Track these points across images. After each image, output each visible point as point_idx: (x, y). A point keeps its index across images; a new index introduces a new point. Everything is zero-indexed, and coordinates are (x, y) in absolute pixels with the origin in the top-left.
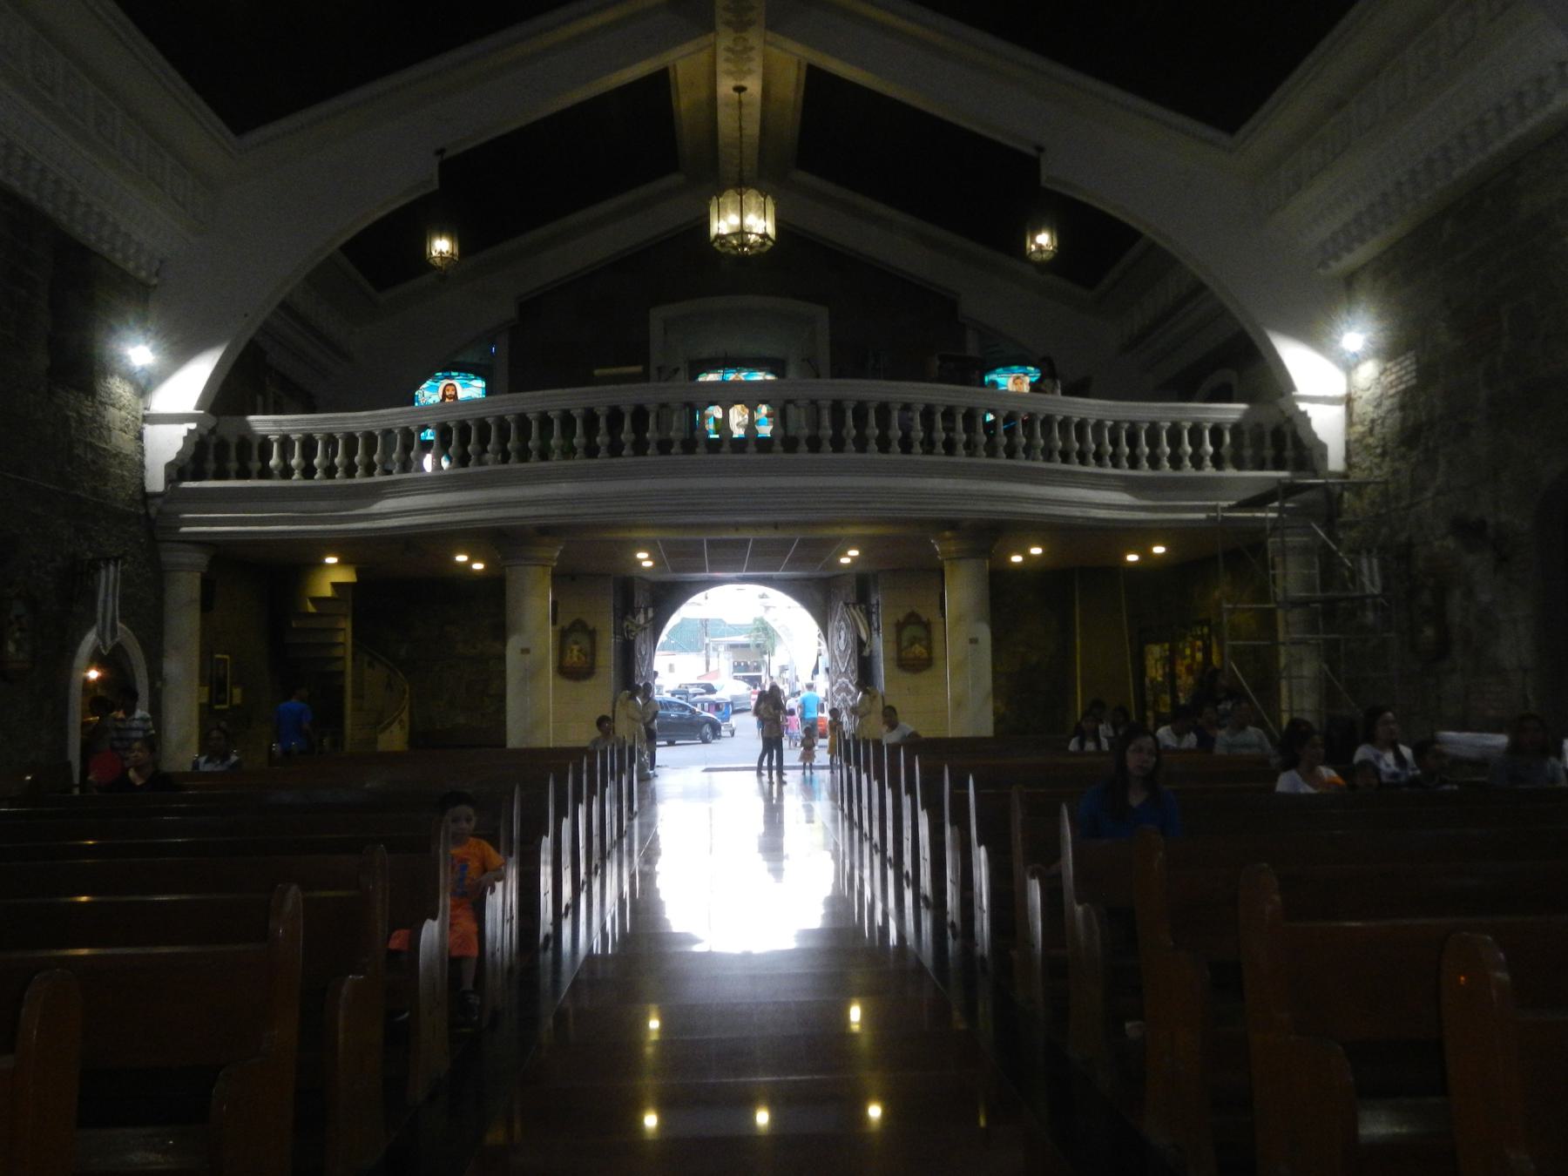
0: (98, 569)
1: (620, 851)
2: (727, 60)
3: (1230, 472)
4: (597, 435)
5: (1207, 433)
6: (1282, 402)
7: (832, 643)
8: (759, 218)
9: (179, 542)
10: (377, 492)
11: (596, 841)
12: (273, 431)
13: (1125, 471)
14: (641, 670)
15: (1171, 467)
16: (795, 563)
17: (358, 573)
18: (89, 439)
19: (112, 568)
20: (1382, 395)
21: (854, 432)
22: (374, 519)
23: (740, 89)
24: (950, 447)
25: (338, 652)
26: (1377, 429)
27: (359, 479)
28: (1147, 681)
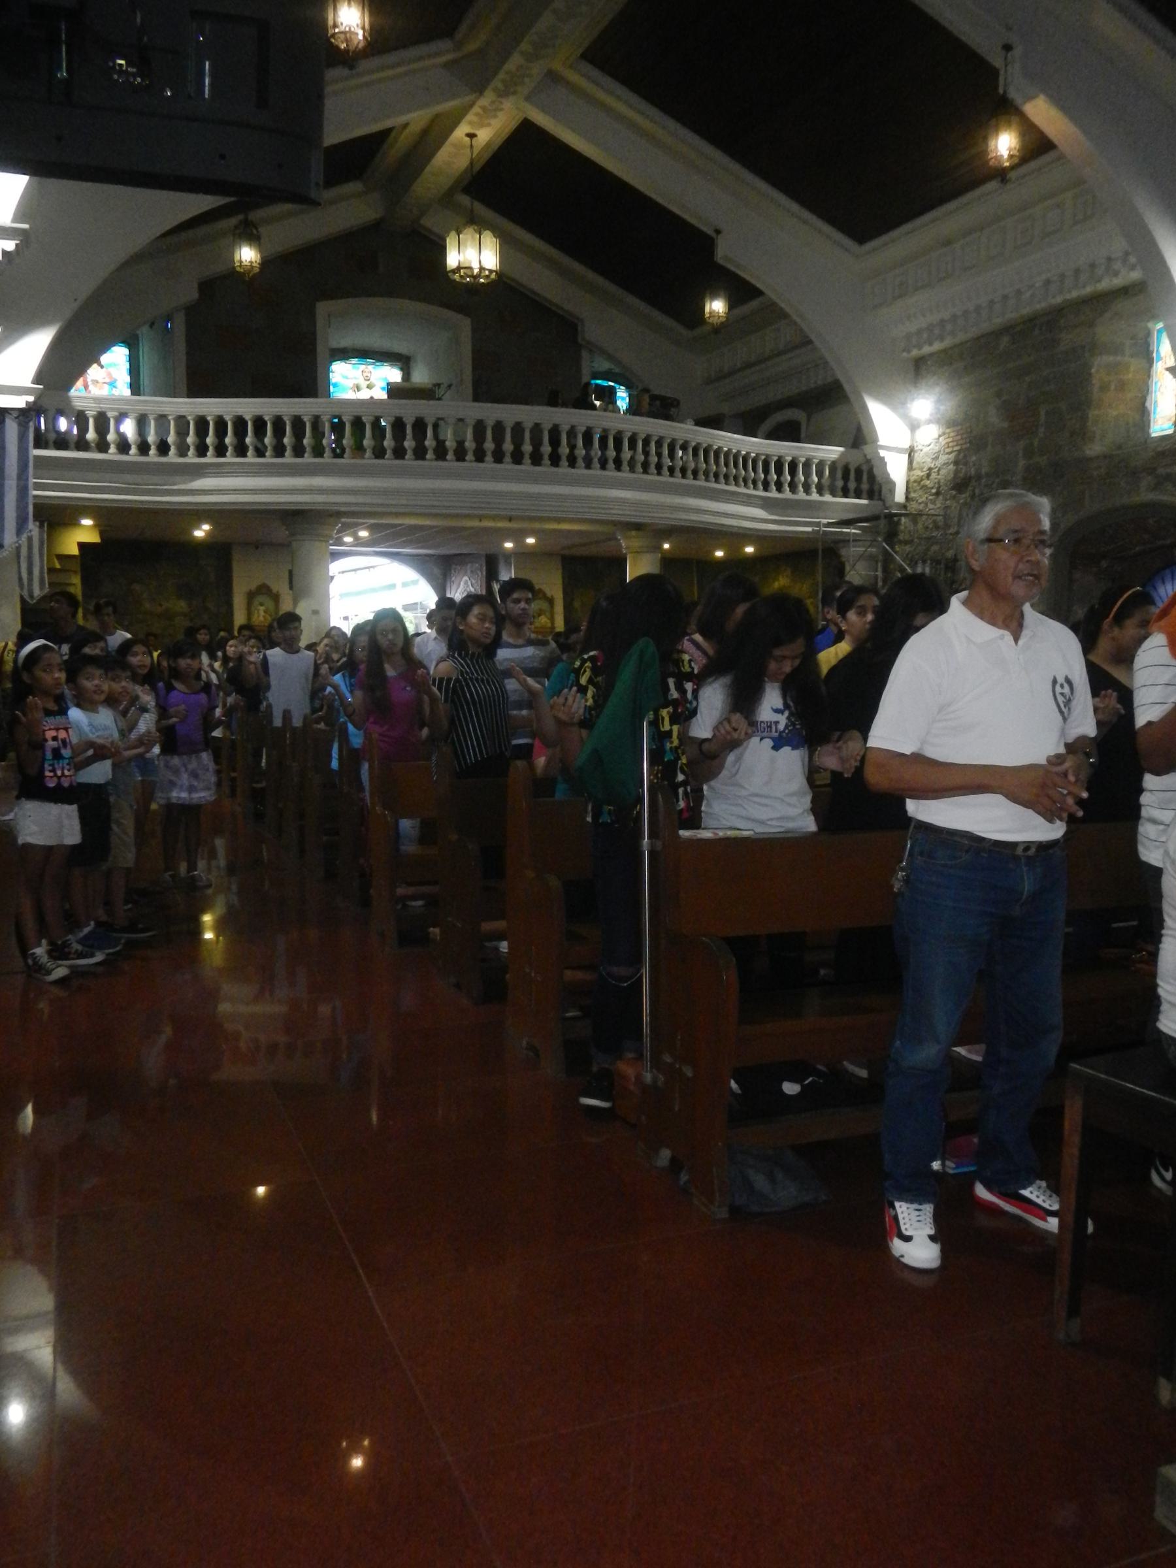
3: (828, 498)
10: (198, 471)
12: (92, 407)
15: (790, 491)
20: (940, 451)
22: (194, 495)
26: (933, 475)
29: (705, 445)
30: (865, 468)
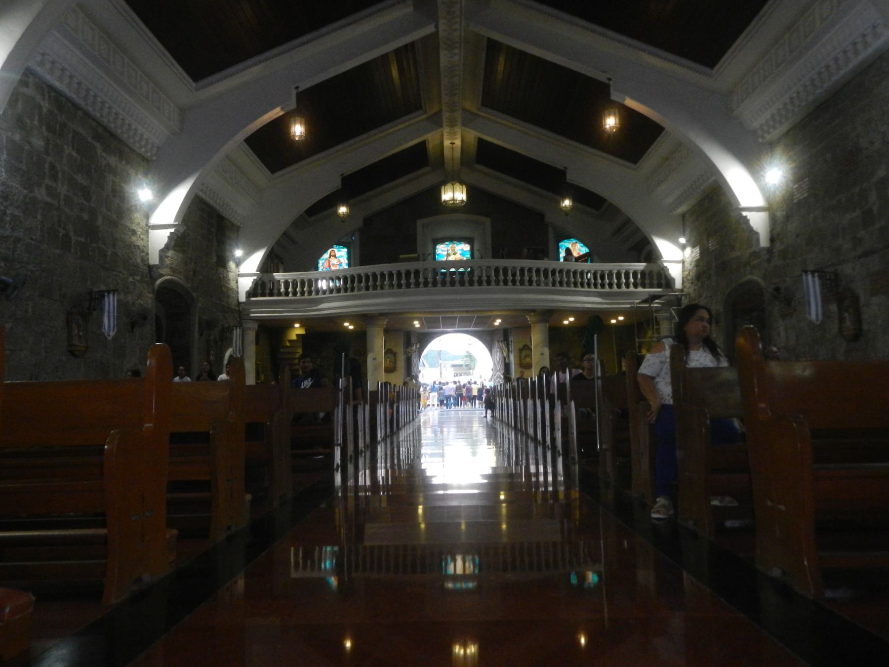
2: (448, 135)
3: (640, 289)
6: (659, 262)
7: (494, 357)
9: (249, 320)
10: (321, 301)
13: (599, 290)
14: (414, 369)
16: (476, 325)
17: (306, 330)
18: (226, 285)
19: (238, 330)
23: (452, 144)
26: (691, 274)
27: (313, 296)
29: (551, 269)
30: (662, 272)
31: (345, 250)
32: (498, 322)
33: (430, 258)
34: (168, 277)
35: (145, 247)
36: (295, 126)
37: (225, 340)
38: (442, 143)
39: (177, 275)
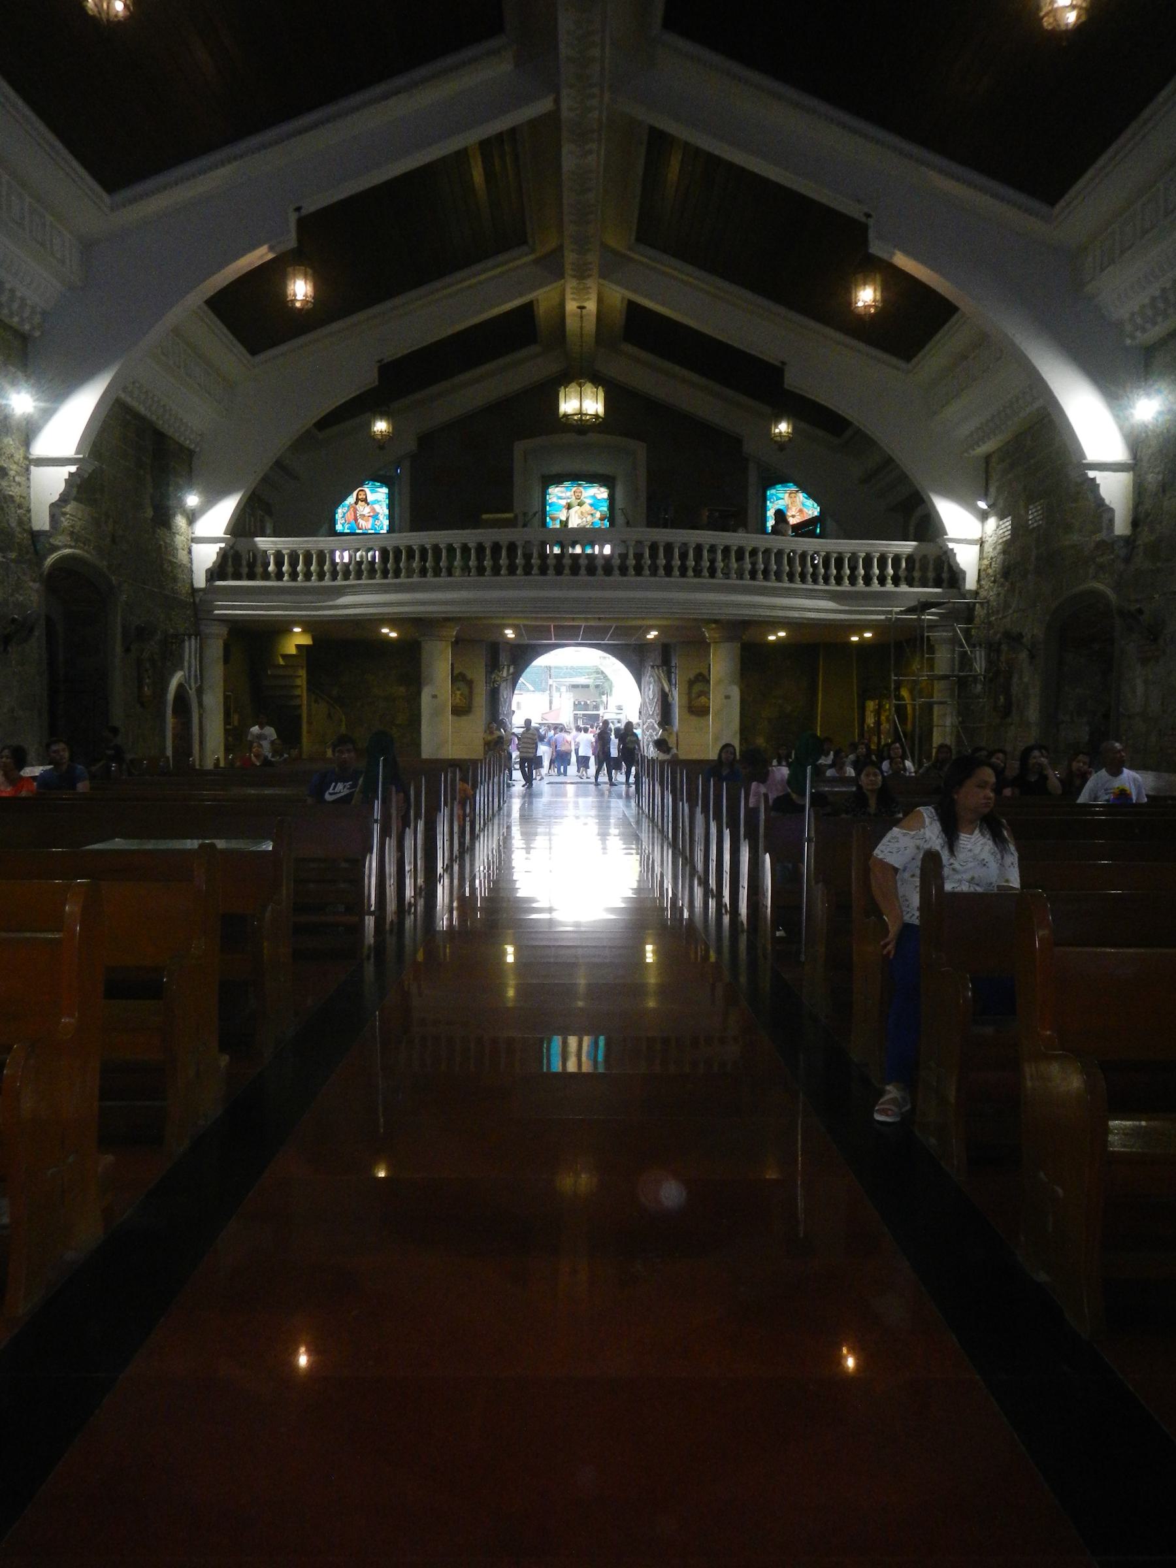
0: (183, 641)
1: (499, 814)
3: (904, 588)
4: (484, 560)
5: (890, 561)
7: (644, 694)
8: (594, 402)
9: (214, 620)
11: (491, 804)
13: (833, 587)
14: (503, 710)
17: (314, 639)
18: (170, 558)
19: (193, 641)
21: (649, 562)
23: (582, 308)
24: (712, 573)
25: (297, 692)
27: (327, 582)
28: (866, 727)
30: (944, 558)
31: (385, 490)
32: (652, 635)
33: (536, 521)
34: (67, 551)
35: (24, 498)
36: (295, 282)
37: (170, 657)
38: (562, 305)
39: (82, 545)
